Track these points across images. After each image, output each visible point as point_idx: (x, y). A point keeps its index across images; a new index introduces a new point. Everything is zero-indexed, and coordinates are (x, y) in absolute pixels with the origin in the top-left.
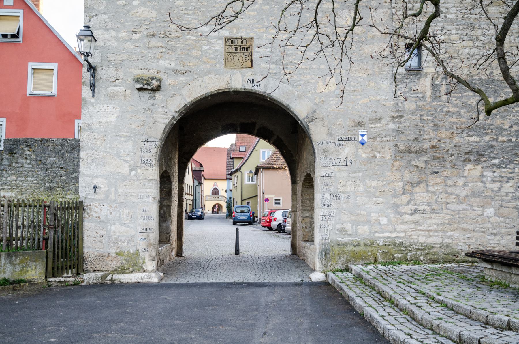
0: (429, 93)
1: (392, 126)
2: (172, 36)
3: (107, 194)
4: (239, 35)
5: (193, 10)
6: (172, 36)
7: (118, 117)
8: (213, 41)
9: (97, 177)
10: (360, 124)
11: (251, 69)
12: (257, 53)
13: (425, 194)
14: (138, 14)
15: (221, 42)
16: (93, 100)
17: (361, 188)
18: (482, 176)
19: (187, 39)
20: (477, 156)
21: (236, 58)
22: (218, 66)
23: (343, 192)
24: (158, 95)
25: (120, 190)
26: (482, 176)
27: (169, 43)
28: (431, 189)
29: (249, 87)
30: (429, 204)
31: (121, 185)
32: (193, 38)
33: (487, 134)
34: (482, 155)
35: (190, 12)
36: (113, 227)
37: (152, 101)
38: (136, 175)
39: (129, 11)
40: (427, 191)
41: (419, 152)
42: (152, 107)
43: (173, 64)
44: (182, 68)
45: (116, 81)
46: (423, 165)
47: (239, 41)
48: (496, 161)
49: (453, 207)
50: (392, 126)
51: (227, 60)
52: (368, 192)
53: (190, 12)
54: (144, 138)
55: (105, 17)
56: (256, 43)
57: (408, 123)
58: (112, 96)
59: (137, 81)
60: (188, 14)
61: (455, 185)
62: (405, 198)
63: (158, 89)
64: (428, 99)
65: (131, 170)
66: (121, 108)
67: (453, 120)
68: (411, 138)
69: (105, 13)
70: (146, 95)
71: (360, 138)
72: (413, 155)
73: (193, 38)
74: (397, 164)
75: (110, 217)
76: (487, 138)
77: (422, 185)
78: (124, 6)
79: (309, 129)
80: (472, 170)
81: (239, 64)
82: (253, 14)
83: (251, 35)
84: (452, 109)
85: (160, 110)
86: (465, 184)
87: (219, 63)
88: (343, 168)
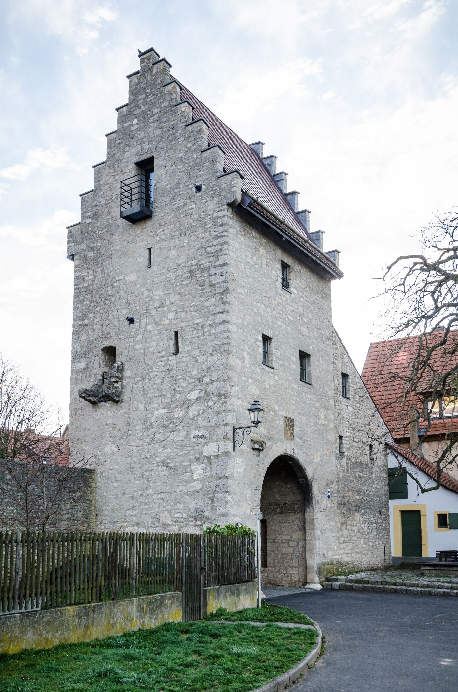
0: (346, 468)
1: (337, 487)
12: (296, 429)
23: (324, 529)
26: (360, 520)
33: (360, 495)
35: (272, 394)
44: (268, 435)
48: (363, 511)
50: (337, 487)
51: (285, 433)
52: (330, 529)
53: (272, 394)
56: (295, 423)
57: (340, 486)
61: (353, 526)
69: (237, 385)
70: (256, 453)
72: (342, 506)
73: (273, 414)
77: (345, 525)
79: (312, 485)
82: (294, 402)
83: (293, 417)
84: (352, 479)
85: (261, 465)
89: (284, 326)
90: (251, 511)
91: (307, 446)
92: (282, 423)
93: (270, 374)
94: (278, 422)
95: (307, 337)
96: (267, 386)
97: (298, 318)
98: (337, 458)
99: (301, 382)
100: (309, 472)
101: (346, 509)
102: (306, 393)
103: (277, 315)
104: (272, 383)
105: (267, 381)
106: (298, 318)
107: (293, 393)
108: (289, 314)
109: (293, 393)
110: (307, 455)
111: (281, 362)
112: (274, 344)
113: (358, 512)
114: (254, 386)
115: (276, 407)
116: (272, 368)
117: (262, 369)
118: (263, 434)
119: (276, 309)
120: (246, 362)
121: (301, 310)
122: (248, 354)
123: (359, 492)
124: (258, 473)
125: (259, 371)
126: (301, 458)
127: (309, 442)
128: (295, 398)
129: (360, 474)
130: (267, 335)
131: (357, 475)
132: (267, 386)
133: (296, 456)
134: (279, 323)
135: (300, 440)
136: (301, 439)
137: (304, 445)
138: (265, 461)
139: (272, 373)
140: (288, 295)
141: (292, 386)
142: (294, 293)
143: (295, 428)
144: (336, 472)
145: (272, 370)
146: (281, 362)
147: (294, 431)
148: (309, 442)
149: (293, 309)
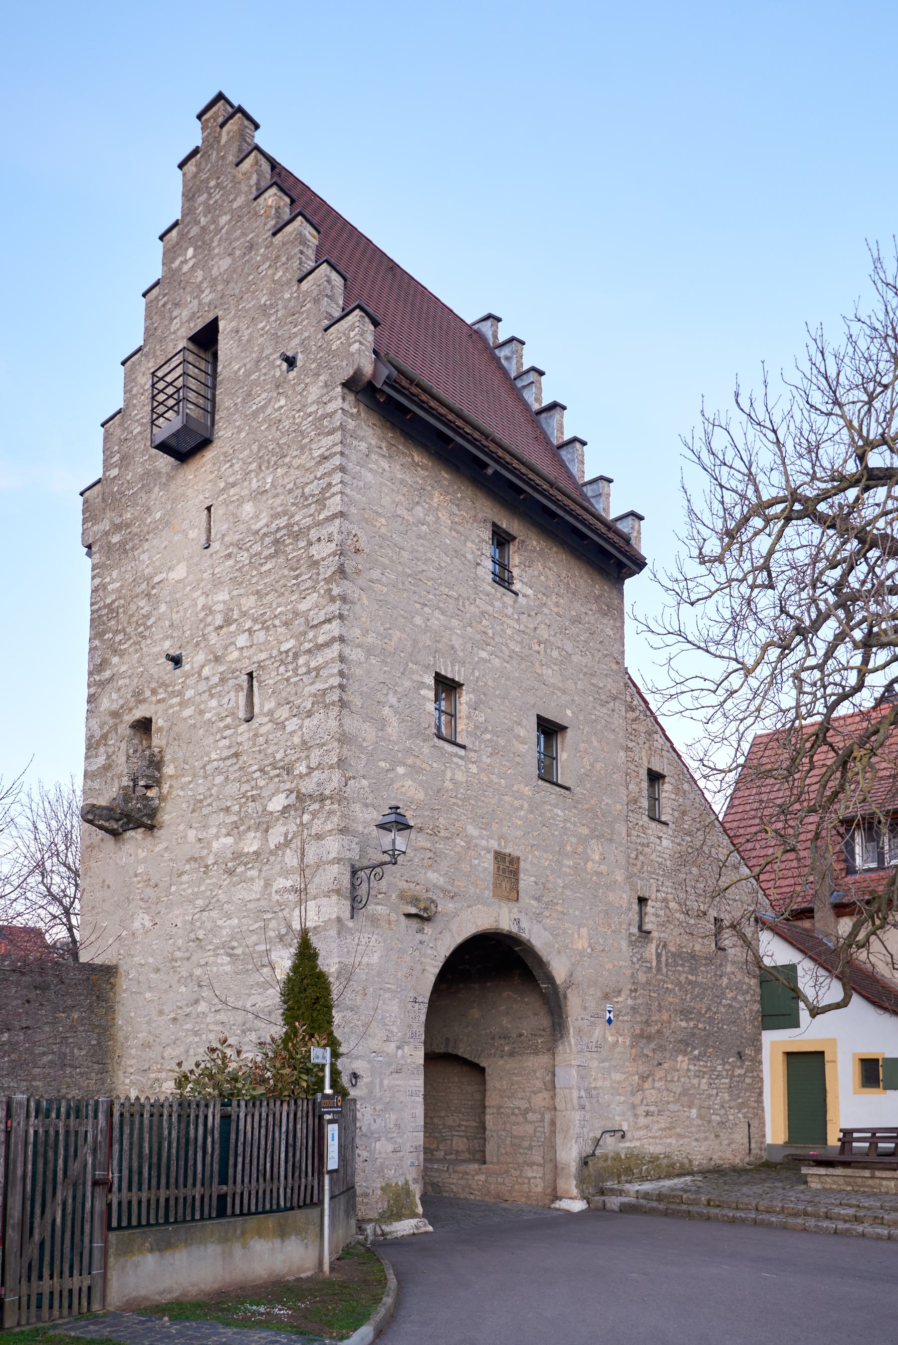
0: (654, 964)
1: (630, 1002)
2: (442, 834)
3: (370, 1086)
4: (507, 851)
5: (462, 800)
6: (442, 834)
7: (381, 957)
8: (483, 853)
9: (357, 1058)
10: (606, 997)
11: (517, 905)
12: (526, 881)
13: (653, 1091)
14: (404, 790)
15: (491, 856)
16: (350, 924)
17: (607, 1083)
18: (688, 1070)
19: (456, 845)
20: (685, 1044)
21: (504, 884)
22: (487, 892)
23: (595, 1088)
24: (428, 929)
25: (386, 1082)
26: (688, 1070)
27: (438, 845)
28: (657, 1085)
29: (515, 929)
30: (656, 1104)
31: (388, 1073)
32: (463, 844)
33: (692, 1019)
34: (688, 1045)
35: (460, 803)
36: (378, 1144)
37: (419, 936)
38: (403, 1057)
39: (392, 781)
40: (653, 1088)
41: (649, 1038)
42: (420, 946)
43: (441, 881)
44: (449, 888)
45: (380, 896)
46: (651, 1054)
47: (507, 859)
48: (696, 1052)
49: (672, 1107)
50: (630, 1002)
52: (613, 1088)
53: (460, 803)
54: (412, 994)
55: (365, 783)
56: (522, 865)
57: (640, 1001)
58: (374, 920)
59: (414, 901)
60: (458, 806)
61: (672, 1081)
62: (639, 1095)
63: (428, 919)
64: (654, 971)
65: (398, 1048)
66: (384, 942)
67: (671, 999)
68: (644, 1018)
69: (364, 777)
70: (415, 924)
71: (608, 1015)
72: (644, 1041)
73: (463, 844)
74: (634, 1050)
75: (374, 1127)
76: (692, 1024)
77: (650, 1080)
78: (388, 771)
80: (682, 1062)
81: (505, 894)
82: (519, 822)
83: (517, 853)
84: (670, 986)
85: (429, 951)
86: (678, 1080)
87: (487, 888)
88: (595, 1055)
89: (497, 662)
90: (398, 1048)
91: (555, 915)
92: (488, 863)
93: (455, 760)
94: (476, 862)
95: (559, 689)
96: (448, 784)
97: (536, 648)
98: (632, 943)
99: (540, 782)
100: (559, 970)
101: (652, 1046)
102: (556, 806)
103: (478, 637)
104: (460, 777)
105: (449, 775)
106: (536, 648)
107: (517, 803)
108: (511, 638)
109: (517, 803)
110: (552, 934)
111: (488, 736)
112: (465, 698)
113: (685, 1053)
114: (410, 782)
115: (472, 830)
116: (463, 747)
117: (434, 746)
118: (435, 885)
119: (474, 624)
120: (389, 730)
121: (544, 633)
122: (396, 712)
123: (685, 1013)
124: (419, 967)
125: (426, 750)
126: (538, 937)
127: (559, 908)
128: (522, 813)
129: (690, 977)
130: (449, 676)
131: (682, 978)
132: (448, 784)
133: (525, 936)
134: (484, 654)
135: (533, 902)
136: (538, 899)
137: (547, 913)
138: (439, 943)
139: (461, 757)
140: (509, 598)
141: (515, 788)
142: (525, 596)
143: (522, 876)
144: (628, 972)
145: (462, 752)
146: (488, 736)
147: (521, 882)
148: (559, 908)
149: (522, 628)
